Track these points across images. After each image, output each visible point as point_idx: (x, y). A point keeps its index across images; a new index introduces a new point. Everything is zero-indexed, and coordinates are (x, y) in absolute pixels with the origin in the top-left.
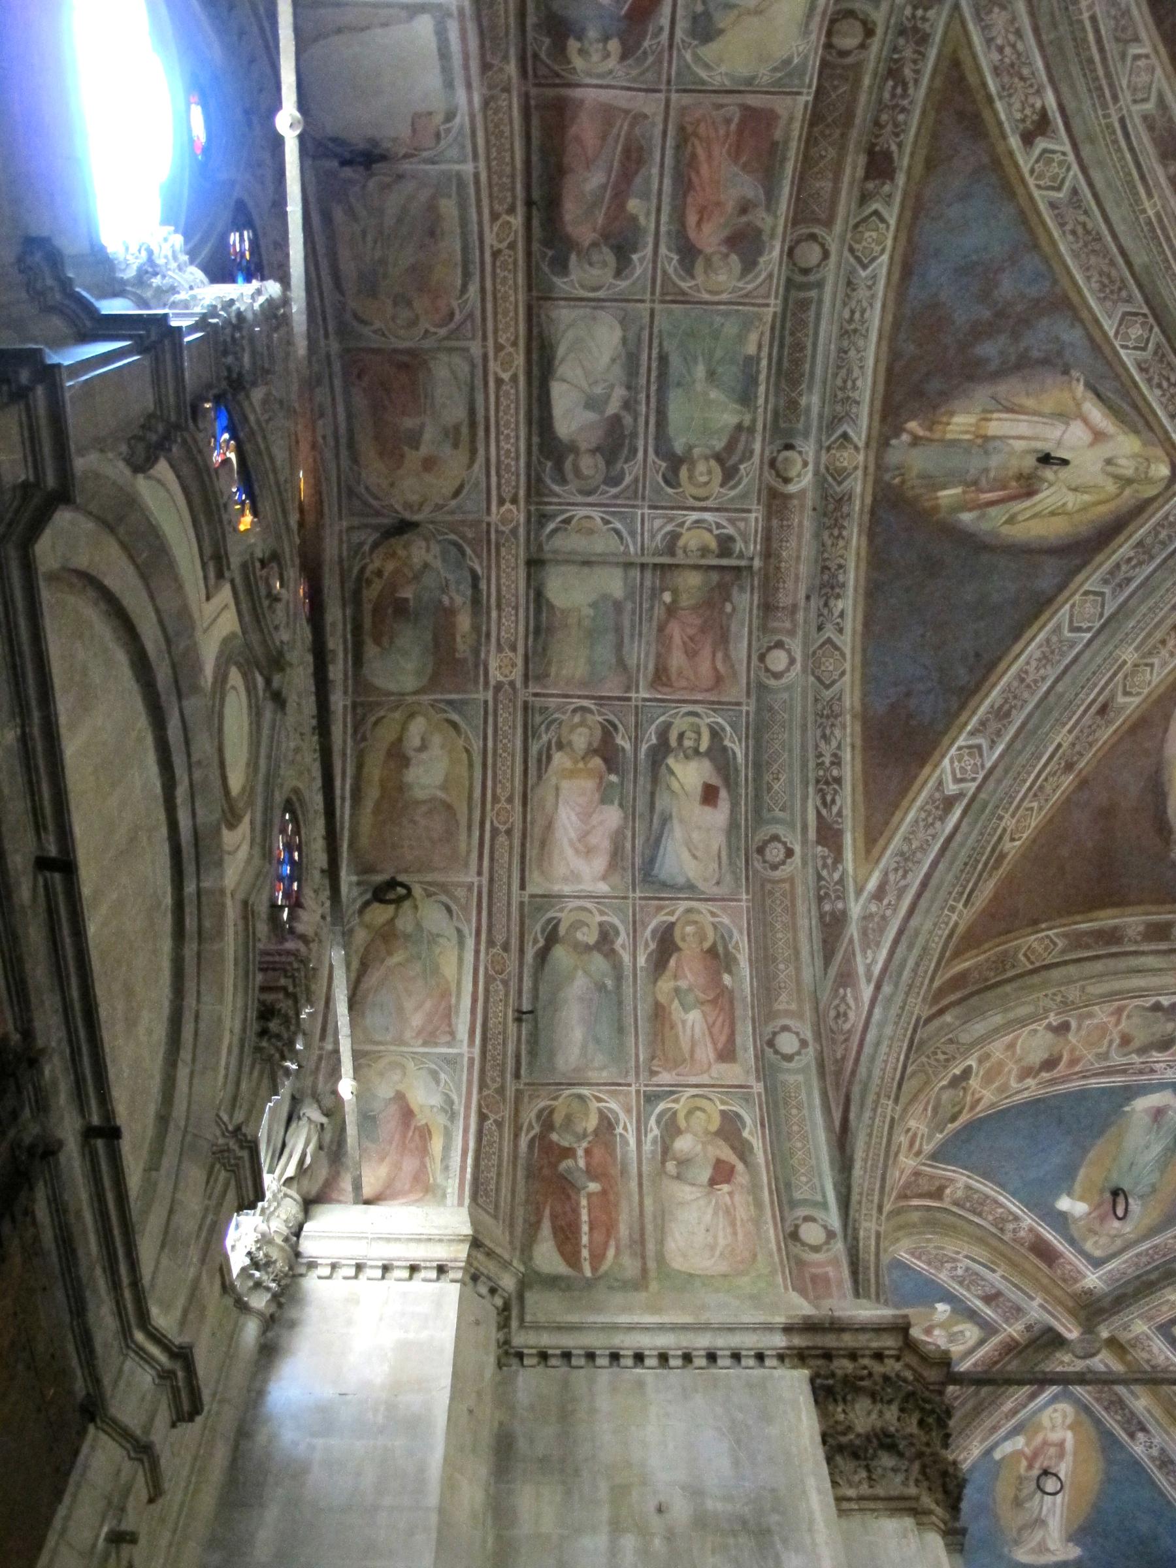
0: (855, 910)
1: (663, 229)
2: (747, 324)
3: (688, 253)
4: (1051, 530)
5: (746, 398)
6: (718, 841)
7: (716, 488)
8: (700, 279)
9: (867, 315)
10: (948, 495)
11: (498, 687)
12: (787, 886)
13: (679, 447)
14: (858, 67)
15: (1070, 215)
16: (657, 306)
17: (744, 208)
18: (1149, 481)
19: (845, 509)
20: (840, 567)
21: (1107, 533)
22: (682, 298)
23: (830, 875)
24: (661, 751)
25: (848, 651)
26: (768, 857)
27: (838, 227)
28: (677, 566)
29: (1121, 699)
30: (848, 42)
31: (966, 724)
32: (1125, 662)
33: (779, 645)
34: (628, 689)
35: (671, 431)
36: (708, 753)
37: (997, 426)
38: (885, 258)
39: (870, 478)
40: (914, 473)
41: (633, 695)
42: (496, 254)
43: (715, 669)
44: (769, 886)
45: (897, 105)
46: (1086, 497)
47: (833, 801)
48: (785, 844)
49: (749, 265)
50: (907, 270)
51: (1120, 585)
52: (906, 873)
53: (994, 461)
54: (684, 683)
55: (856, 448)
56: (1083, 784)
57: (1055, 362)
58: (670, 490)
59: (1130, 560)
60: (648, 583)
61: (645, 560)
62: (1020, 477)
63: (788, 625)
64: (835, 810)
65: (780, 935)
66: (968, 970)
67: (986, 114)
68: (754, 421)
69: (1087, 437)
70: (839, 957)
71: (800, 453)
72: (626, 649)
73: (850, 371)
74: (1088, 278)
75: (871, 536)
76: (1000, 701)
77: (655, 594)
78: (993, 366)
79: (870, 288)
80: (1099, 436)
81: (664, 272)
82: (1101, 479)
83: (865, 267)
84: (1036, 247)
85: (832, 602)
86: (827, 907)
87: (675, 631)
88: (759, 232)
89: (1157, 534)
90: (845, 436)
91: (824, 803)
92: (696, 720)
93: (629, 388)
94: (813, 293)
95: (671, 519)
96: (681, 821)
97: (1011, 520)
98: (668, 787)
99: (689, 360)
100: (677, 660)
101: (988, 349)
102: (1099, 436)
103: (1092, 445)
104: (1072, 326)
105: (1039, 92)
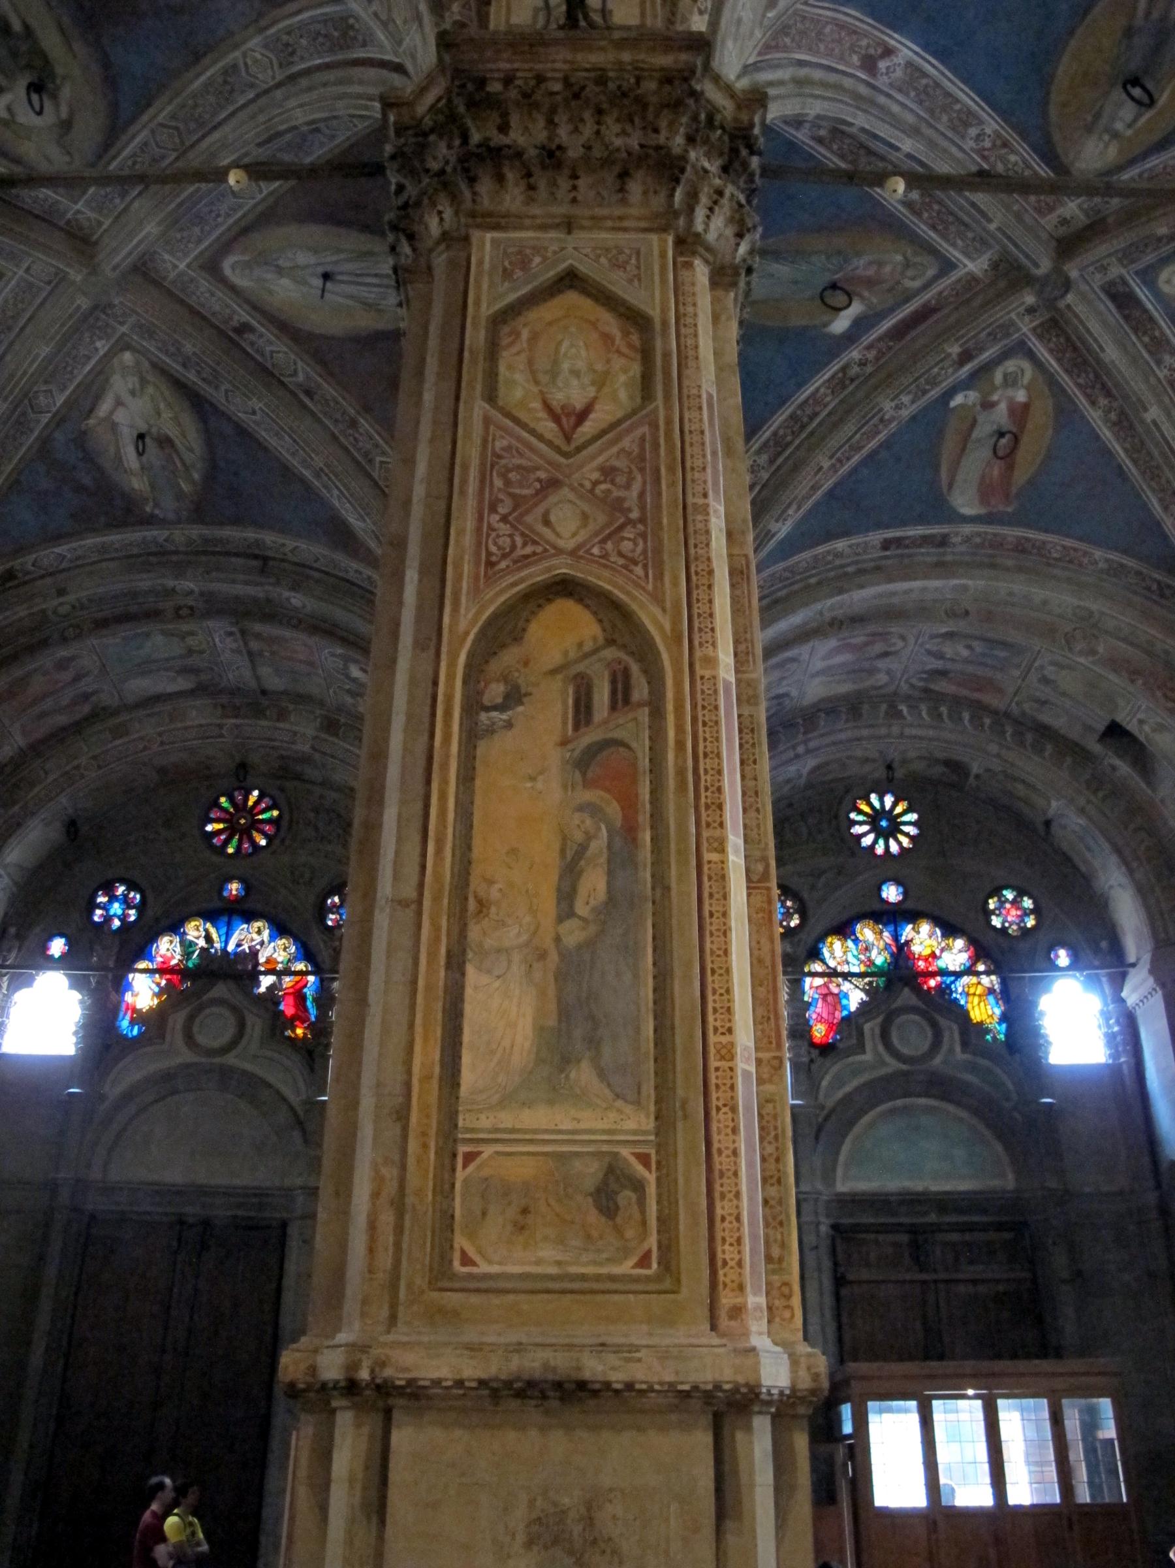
3: (77, 678)
4: (189, 422)
11: (313, 748)
18: (138, 363)
29: (301, 377)
42: (100, 767)
46: (162, 406)
50: (58, 538)
57: (81, 440)
59: (198, 372)
69: (121, 410)
80: (119, 403)
97: (191, 450)
101: (87, 480)
102: (119, 403)
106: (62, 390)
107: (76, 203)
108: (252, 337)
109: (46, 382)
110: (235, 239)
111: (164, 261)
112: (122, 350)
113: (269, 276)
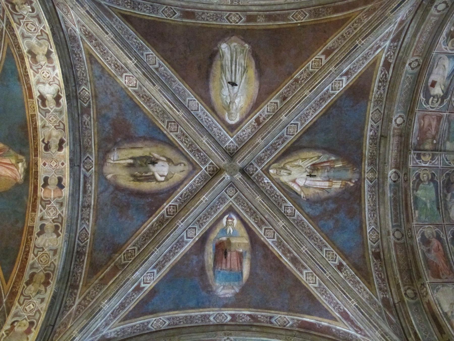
0: (388, 43)
1: (447, 244)
2: (419, 219)
3: (439, 238)
5: (416, 198)
6: (435, 71)
7: (422, 173)
8: (434, 231)
9: (370, 215)
10: (339, 165)
12: (415, 54)
13: (432, 185)
14: (404, 286)
15: (320, 244)
16: (443, 223)
17: (429, 251)
18: (275, 168)
19: (370, 161)
20: (371, 144)
21: (287, 153)
22: (437, 225)
23: (390, 53)
24: (443, 98)
25: (370, 119)
26: (417, 63)
27: (392, 243)
28: (432, 151)
29: (278, 101)
30: (409, 292)
31: (335, 97)
32: (285, 116)
33: (398, 125)
34: (449, 115)
35: (434, 189)
36: (431, 96)
37: (326, 184)
38: (368, 231)
39: (363, 170)
40: (350, 171)
41: (448, 114)
43: (424, 121)
44: (421, 55)
45: (379, 271)
46: (296, 164)
47: (383, 76)
48: (411, 67)
49: (423, 235)
50: (361, 228)
51: (281, 137)
52: (367, 54)
53: (326, 174)
54: (433, 117)
55: (368, 178)
56: (290, 74)
57: (311, 202)
58: (433, 172)
59: (279, 145)
60: (440, 146)
61: (440, 153)
62: (318, 170)
63: (395, 131)
64: (383, 73)
65: (424, 40)
66: (334, 13)
67: (356, 271)
68: (413, 192)
69: (297, 181)
70: (400, 29)
71: (392, 180)
72: (448, 127)
73: (372, 200)
74: (308, 226)
75: (362, 153)
76: (323, 103)
77: (438, 143)
78: (330, 201)
79: (370, 223)
80: (294, 181)
81: (443, 232)
82: (291, 169)
83: (373, 228)
84: (326, 235)
85: (374, 134)
86: (396, 44)
87: (433, 132)
88: (423, 244)
89: (271, 152)
90: (371, 182)
91: (386, 75)
92: (432, 106)
93: (446, 201)
94: (394, 224)
95: (433, 164)
96: (444, 77)
97: (319, 157)
98: (445, 87)
99: (431, 208)
100: (434, 123)
101: (332, 206)
102: (294, 181)
103: (296, 179)
104: (309, 212)
105: (345, 277)
106: (286, 202)
107: (202, 169)
108: (261, 119)
109: (281, 207)
110: (218, 116)
111: (229, 146)
112: (268, 172)
113: (234, 107)
